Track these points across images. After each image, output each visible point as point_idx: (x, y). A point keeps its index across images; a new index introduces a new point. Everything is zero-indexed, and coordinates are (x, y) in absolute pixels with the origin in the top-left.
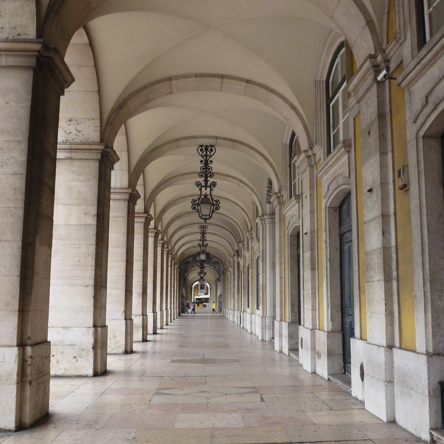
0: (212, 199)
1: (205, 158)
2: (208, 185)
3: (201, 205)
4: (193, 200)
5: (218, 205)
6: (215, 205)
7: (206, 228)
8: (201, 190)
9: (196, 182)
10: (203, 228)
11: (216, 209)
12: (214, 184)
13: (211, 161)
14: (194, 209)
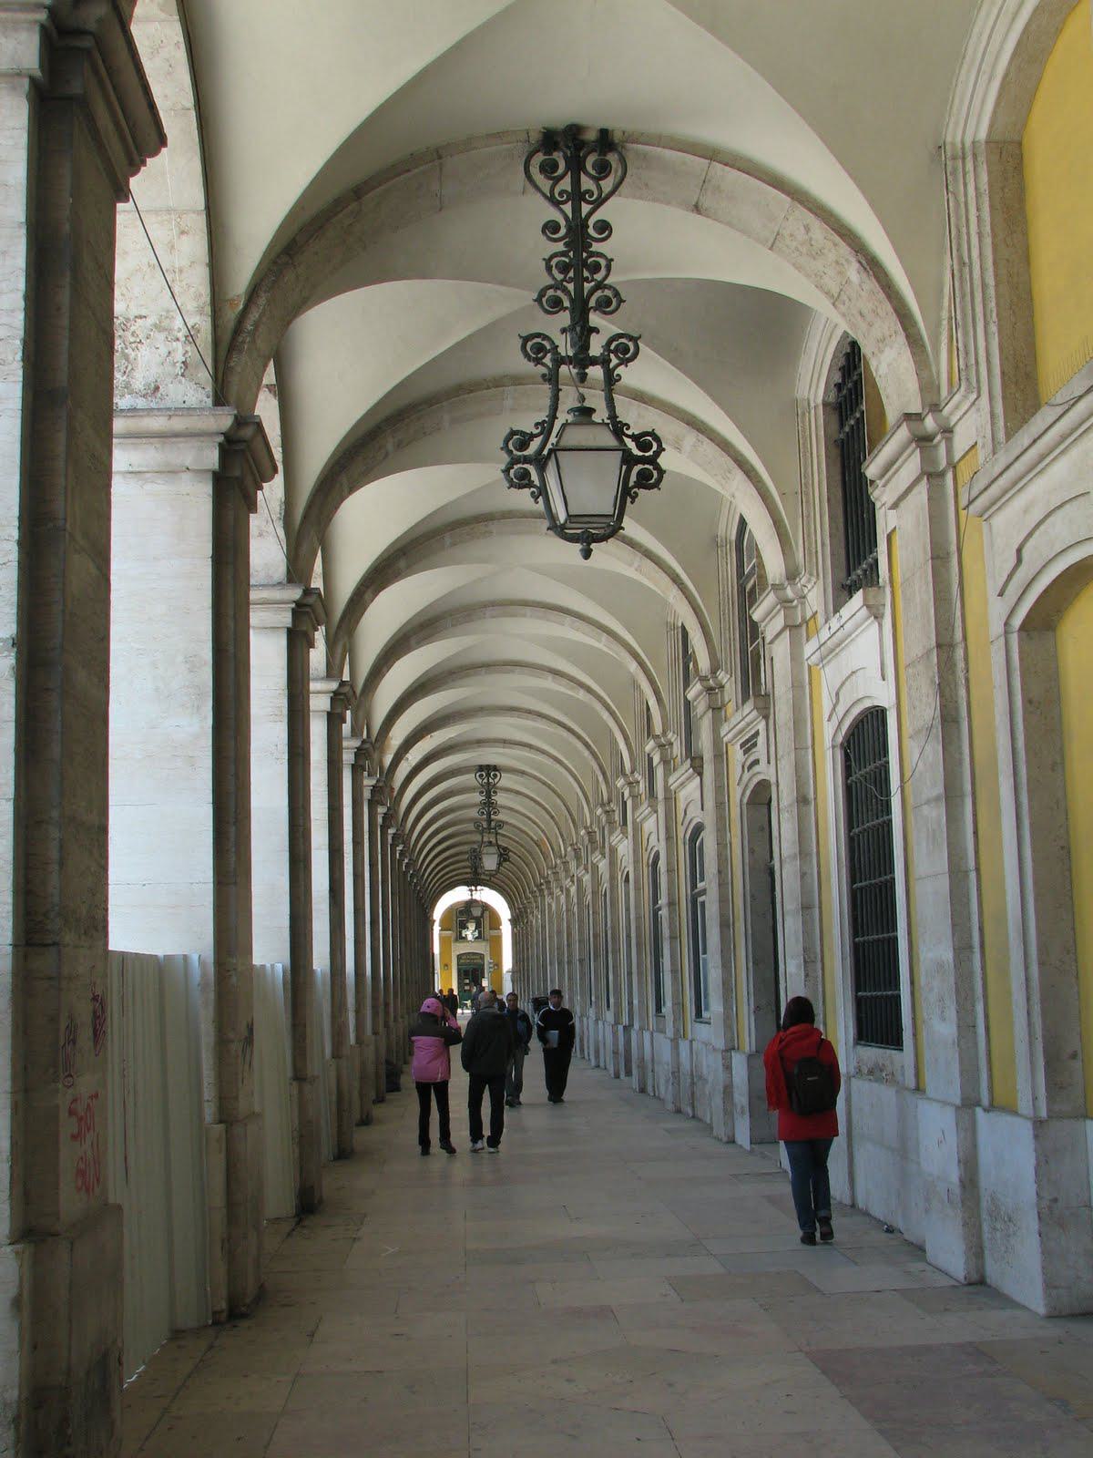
0: (618, 429)
1: (568, 208)
2: (596, 349)
4: (513, 433)
5: (652, 461)
7: (495, 776)
8: (552, 378)
9: (526, 339)
10: (488, 775)
11: (645, 481)
12: (624, 349)
13: (604, 227)
14: (521, 487)
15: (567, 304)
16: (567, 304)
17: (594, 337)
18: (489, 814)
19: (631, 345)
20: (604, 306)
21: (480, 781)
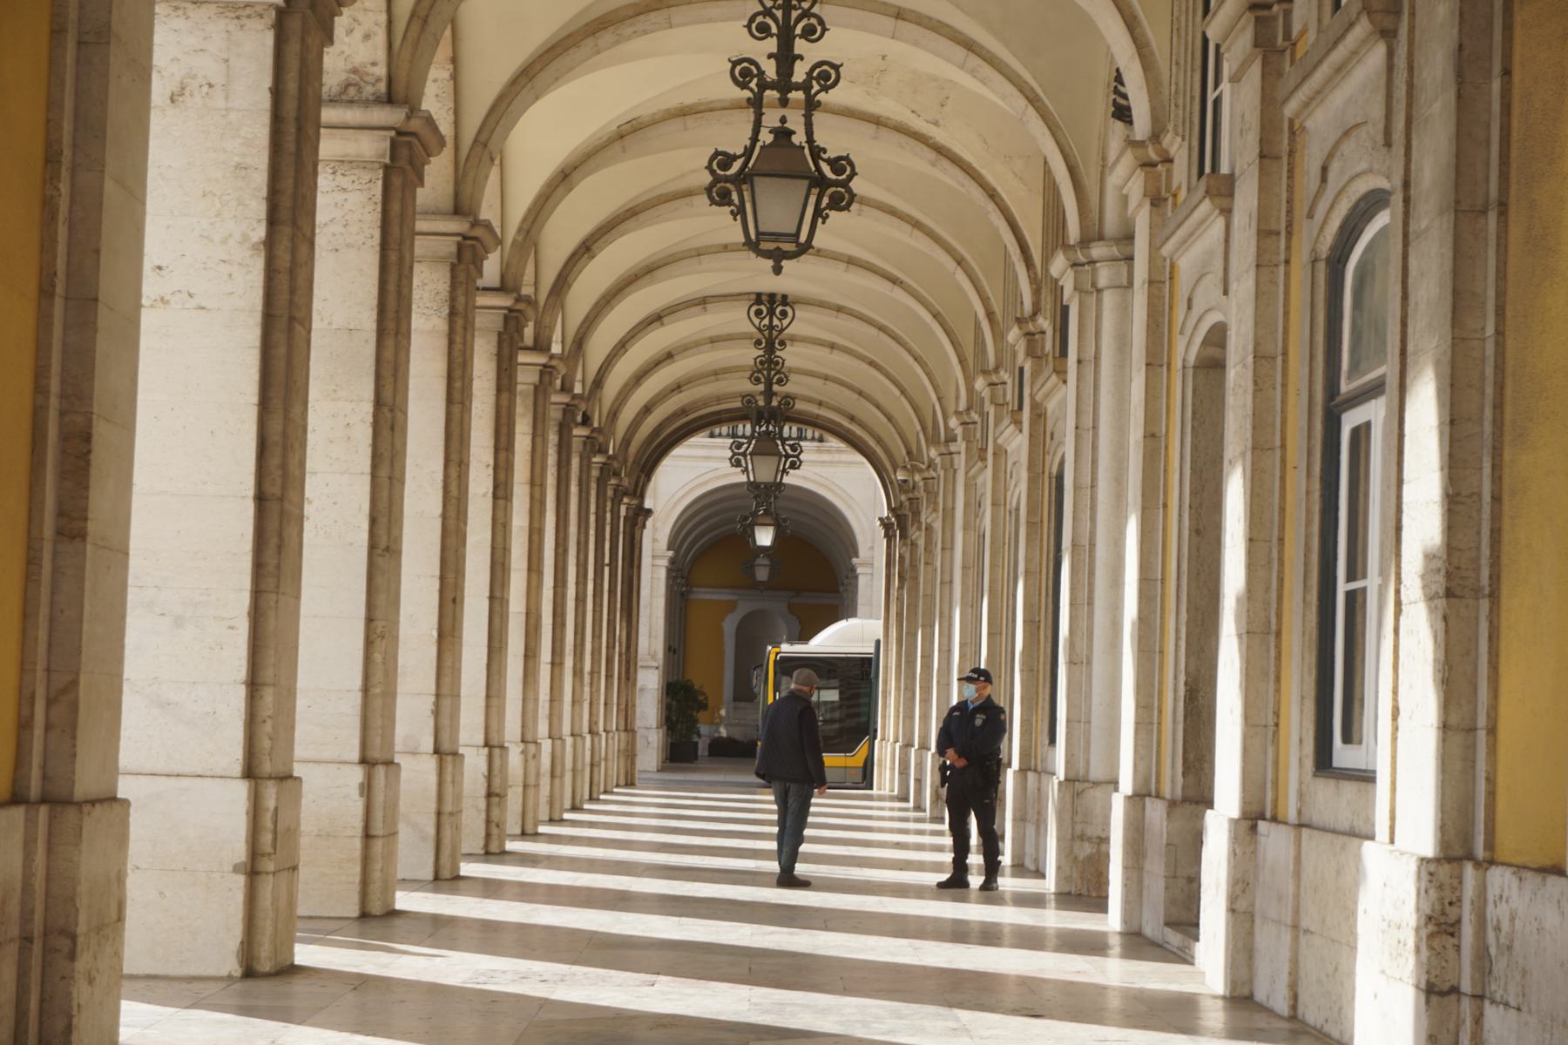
0: (817, 152)
2: (799, 74)
3: (757, 180)
4: (717, 153)
5: (845, 184)
6: (831, 186)
8: (756, 103)
9: (735, 64)
10: (771, 313)
12: (827, 75)
14: (720, 204)
15: (774, 30)
16: (774, 30)
17: (798, 62)
18: (769, 384)
19: (832, 72)
20: (808, 33)
21: (756, 321)
